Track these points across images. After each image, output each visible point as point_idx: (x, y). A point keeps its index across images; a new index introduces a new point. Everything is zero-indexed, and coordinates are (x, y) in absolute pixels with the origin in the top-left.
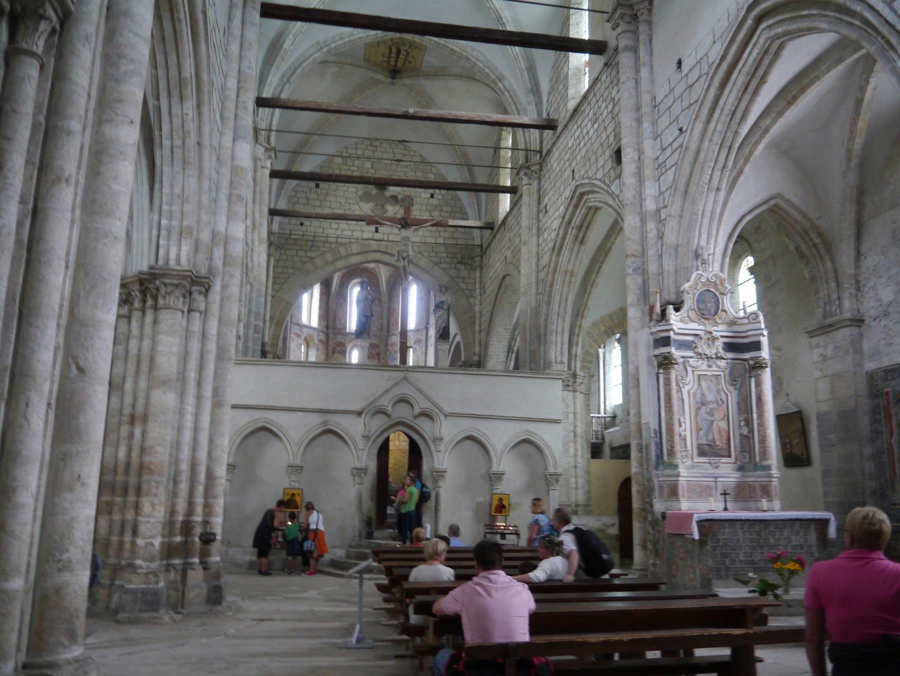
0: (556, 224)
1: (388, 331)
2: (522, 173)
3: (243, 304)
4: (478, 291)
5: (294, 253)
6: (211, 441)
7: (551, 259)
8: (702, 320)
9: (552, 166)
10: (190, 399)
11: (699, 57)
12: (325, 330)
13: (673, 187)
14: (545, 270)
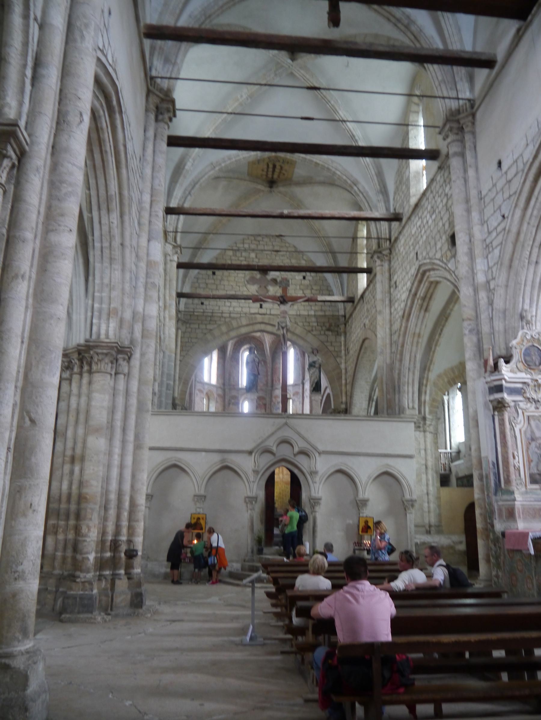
0: (404, 296)
2: (375, 257)
3: (158, 367)
4: (343, 352)
5: (197, 326)
6: (133, 476)
7: (401, 325)
8: (529, 370)
9: (399, 250)
10: (117, 443)
11: (515, 158)
12: (222, 386)
13: (500, 263)
14: (397, 334)
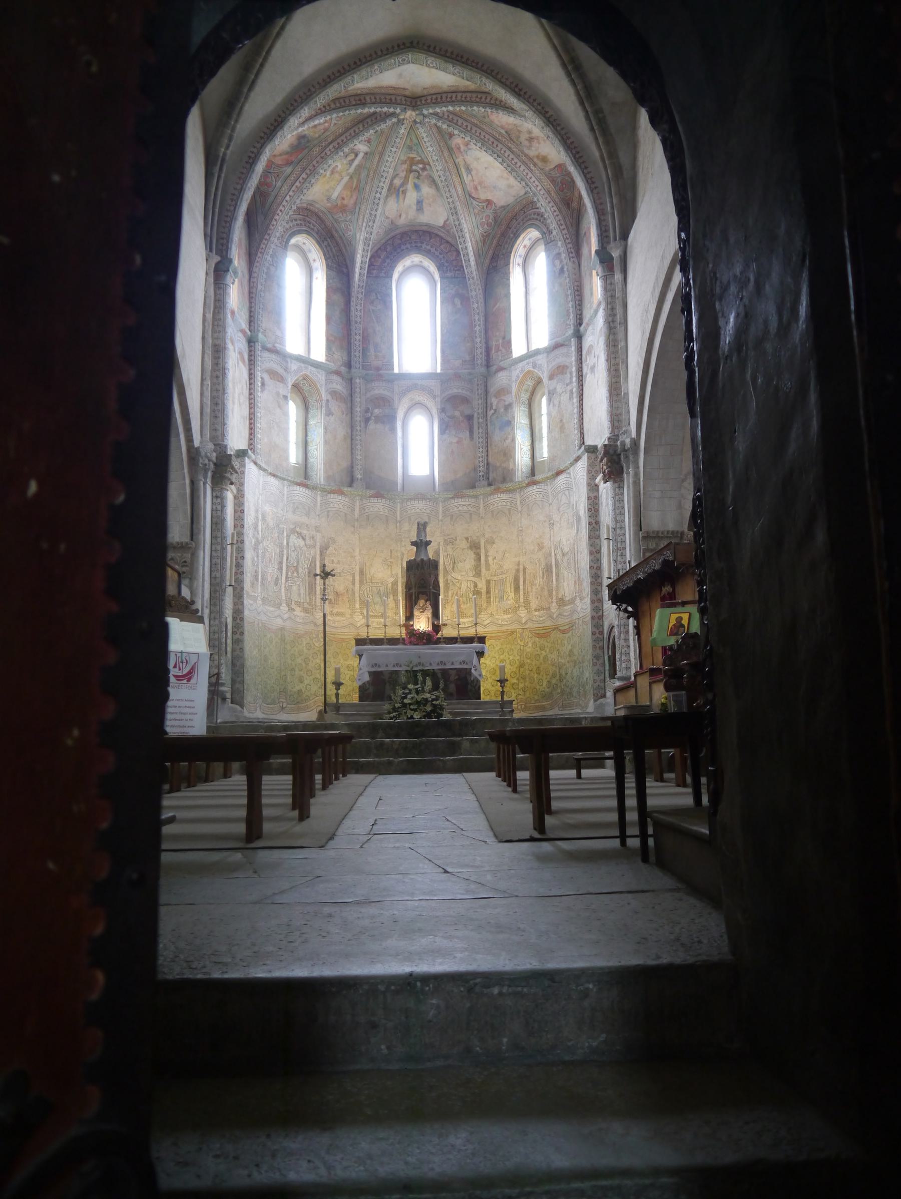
1: (488, 366)
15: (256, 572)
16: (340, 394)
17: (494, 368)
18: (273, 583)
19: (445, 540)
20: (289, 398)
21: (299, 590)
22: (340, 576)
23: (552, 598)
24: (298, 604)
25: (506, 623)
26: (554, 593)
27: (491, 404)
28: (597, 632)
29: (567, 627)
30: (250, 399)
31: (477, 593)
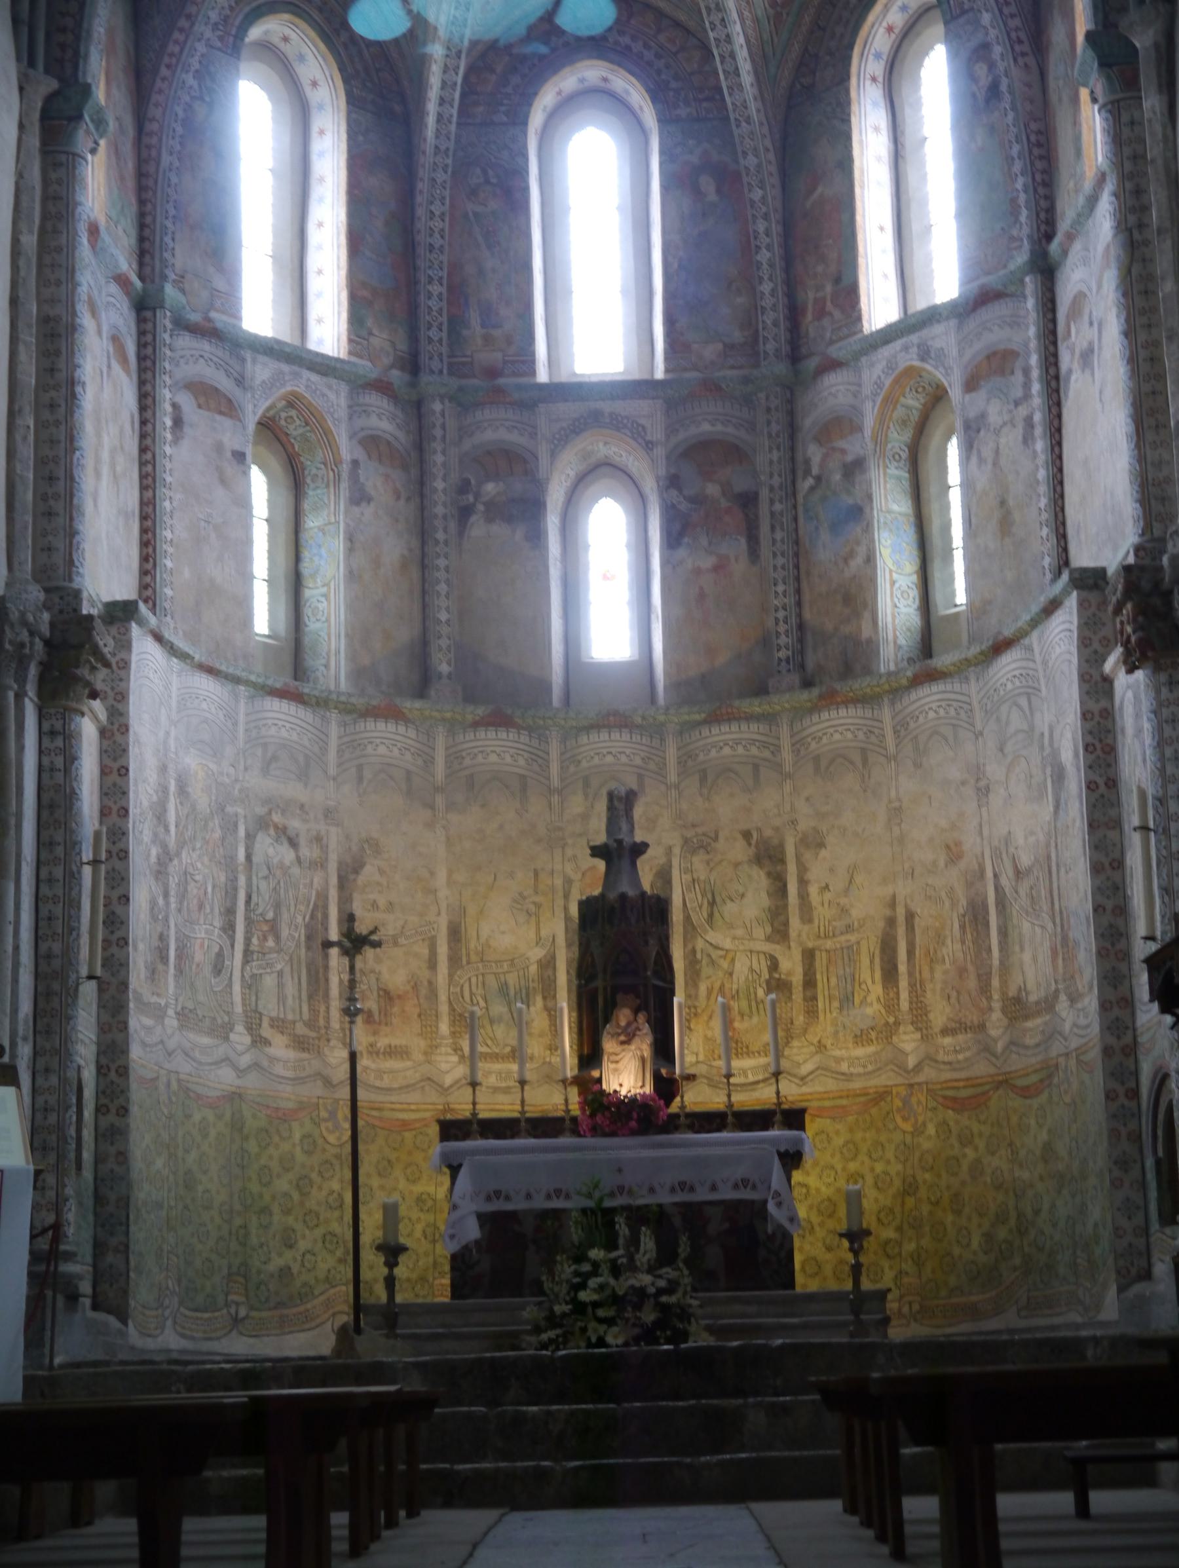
1: (795, 356)
15: (162, 938)
16: (389, 443)
17: (812, 363)
18: (207, 970)
19: (686, 841)
20: (249, 457)
21: (280, 985)
22: (396, 944)
23: (989, 998)
24: (279, 1025)
25: (861, 1070)
26: (995, 982)
27: (807, 462)
28: (1121, 1091)
29: (1034, 1078)
30: (142, 464)
31: (779, 985)
